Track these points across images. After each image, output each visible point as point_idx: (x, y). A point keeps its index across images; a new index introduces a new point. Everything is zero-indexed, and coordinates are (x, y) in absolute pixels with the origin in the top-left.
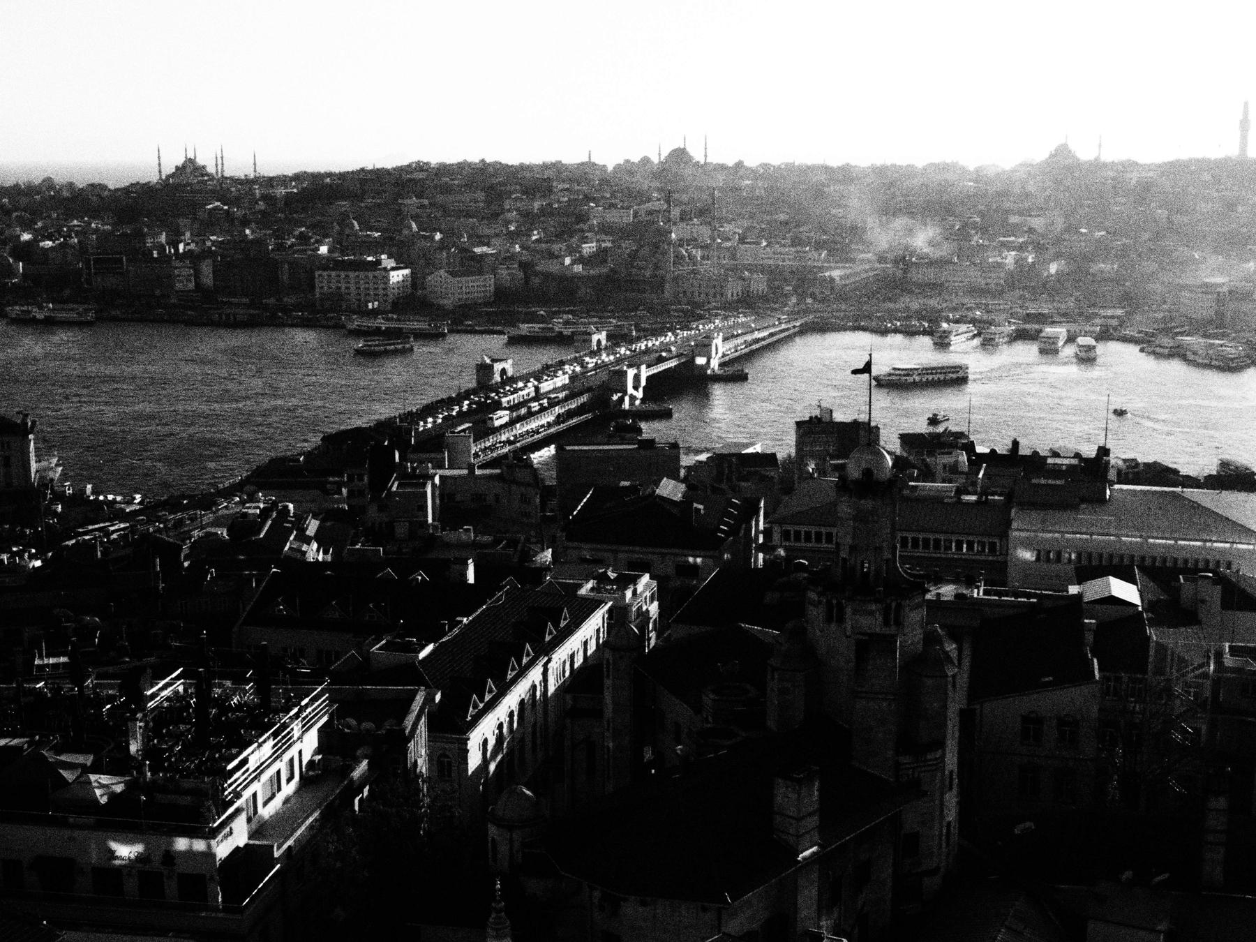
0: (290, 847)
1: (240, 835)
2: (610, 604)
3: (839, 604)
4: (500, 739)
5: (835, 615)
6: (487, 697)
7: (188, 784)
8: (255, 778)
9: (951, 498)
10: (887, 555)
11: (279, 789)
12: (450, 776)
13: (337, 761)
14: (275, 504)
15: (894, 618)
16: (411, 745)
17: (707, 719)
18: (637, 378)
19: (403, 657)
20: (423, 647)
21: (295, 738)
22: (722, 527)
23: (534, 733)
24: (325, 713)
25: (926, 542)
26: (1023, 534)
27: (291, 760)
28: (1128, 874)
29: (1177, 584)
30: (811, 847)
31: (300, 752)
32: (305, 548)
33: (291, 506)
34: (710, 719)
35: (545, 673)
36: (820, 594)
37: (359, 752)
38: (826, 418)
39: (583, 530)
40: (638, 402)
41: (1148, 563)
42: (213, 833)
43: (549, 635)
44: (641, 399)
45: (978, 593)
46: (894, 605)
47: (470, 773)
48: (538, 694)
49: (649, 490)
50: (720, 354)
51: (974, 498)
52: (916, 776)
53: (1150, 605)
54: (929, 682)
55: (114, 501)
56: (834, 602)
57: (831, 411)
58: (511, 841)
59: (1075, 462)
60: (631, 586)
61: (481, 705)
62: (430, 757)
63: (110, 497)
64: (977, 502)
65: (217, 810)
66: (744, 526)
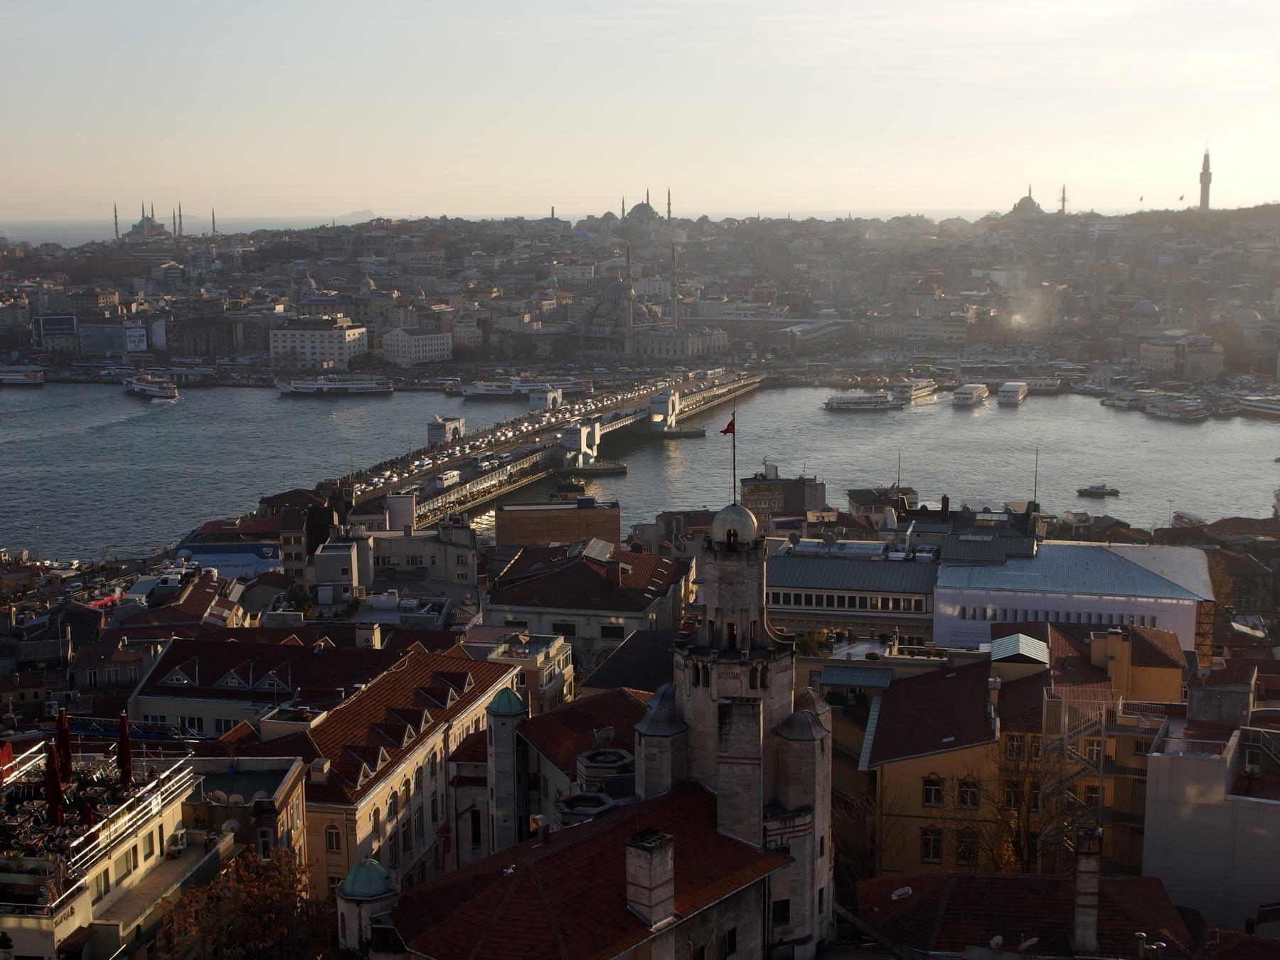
0: (138, 926)
1: (82, 915)
2: (519, 668)
3: (705, 667)
4: (393, 811)
5: (701, 678)
6: (380, 765)
7: (31, 863)
8: (105, 854)
9: (879, 555)
10: (754, 616)
11: (136, 867)
12: (338, 848)
13: (202, 835)
14: (198, 569)
15: (759, 680)
16: (283, 816)
17: (581, 786)
18: (591, 436)
19: (295, 726)
20: (316, 715)
21: (154, 812)
22: (649, 587)
23: (434, 803)
24: (189, 786)
25: (819, 600)
26: (949, 591)
27: (151, 835)
28: (998, 939)
29: (1088, 641)
30: (665, 918)
31: (161, 827)
32: (226, 613)
33: (215, 571)
35: (446, 740)
36: (686, 658)
37: (224, 826)
38: (771, 476)
39: (506, 591)
40: (592, 461)
41: (1062, 619)
42: (53, 912)
43: (451, 700)
44: (596, 457)
45: (892, 652)
46: (760, 668)
47: (358, 843)
48: (438, 759)
49: (576, 552)
50: (677, 412)
51: (902, 555)
52: (784, 842)
53: (1057, 662)
54: (796, 745)
55: (50, 568)
56: (700, 666)
57: (776, 467)
58: (360, 913)
59: (1004, 517)
60: (544, 649)
61: (373, 774)
62: (310, 830)
63: (47, 563)
64: (906, 560)
65: (58, 889)
66: (672, 586)
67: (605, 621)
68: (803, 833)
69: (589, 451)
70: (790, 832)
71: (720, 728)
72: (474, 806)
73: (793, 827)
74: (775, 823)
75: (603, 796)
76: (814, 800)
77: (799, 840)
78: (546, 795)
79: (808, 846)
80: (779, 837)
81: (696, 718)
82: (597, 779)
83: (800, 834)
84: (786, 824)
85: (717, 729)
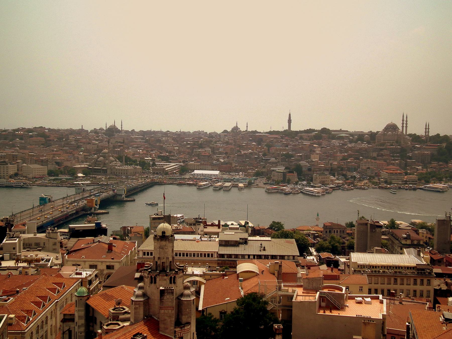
3: (155, 277)
5: (153, 281)
23: (51, 329)
34: (112, 320)
46: (173, 277)
52: (181, 335)
56: (153, 276)
67: (108, 264)
68: (187, 332)
69: (96, 206)
70: (183, 332)
71: (161, 297)
72: (70, 329)
73: (184, 330)
74: (179, 328)
75: (120, 323)
76: (191, 320)
77: (186, 334)
78: (96, 323)
79: (189, 336)
80: (180, 333)
81: (151, 294)
82: (116, 317)
83: (186, 332)
84: (182, 329)
85: (159, 298)
